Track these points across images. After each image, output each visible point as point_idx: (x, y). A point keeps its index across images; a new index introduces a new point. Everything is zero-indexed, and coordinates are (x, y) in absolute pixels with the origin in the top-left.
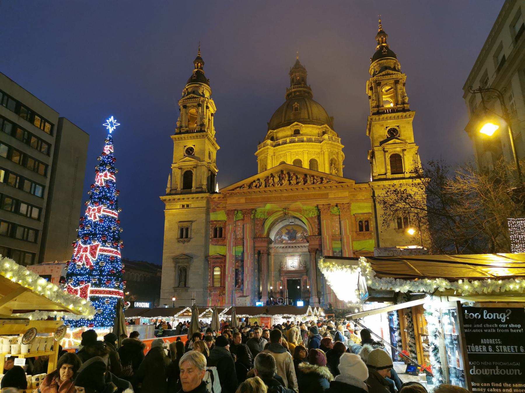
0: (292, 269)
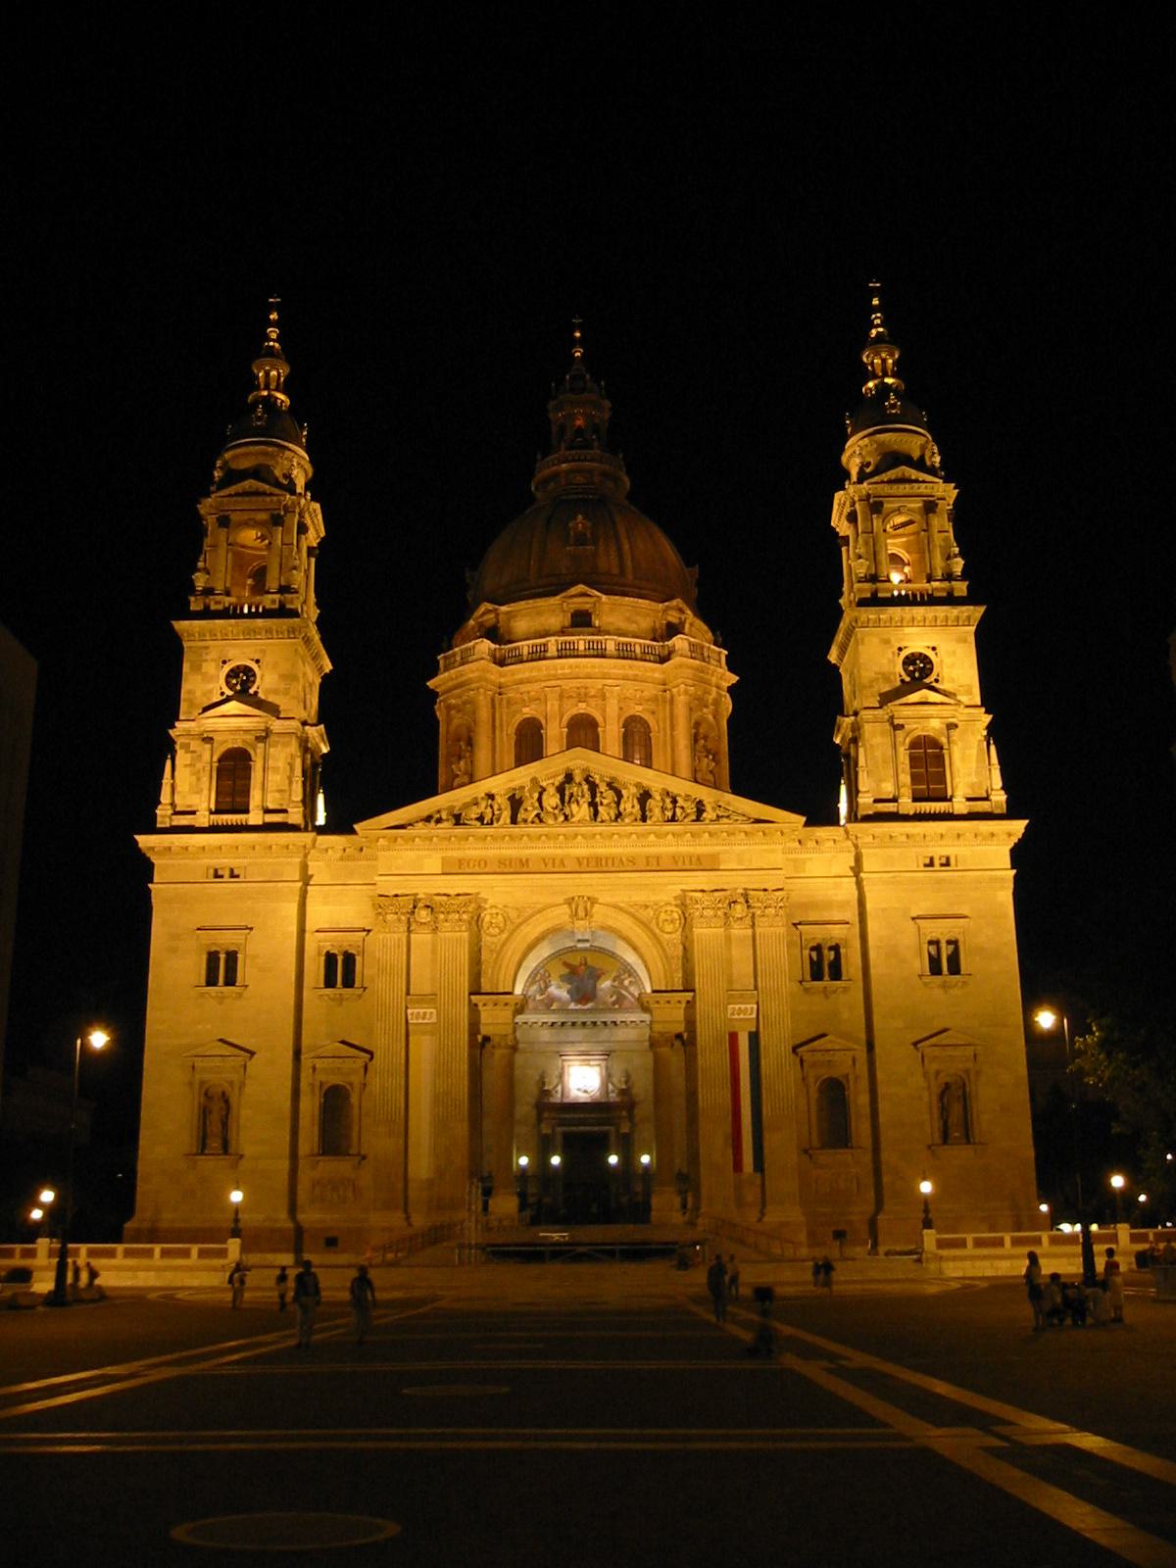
0: (583, 1098)
